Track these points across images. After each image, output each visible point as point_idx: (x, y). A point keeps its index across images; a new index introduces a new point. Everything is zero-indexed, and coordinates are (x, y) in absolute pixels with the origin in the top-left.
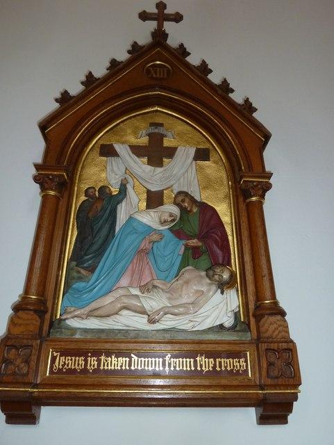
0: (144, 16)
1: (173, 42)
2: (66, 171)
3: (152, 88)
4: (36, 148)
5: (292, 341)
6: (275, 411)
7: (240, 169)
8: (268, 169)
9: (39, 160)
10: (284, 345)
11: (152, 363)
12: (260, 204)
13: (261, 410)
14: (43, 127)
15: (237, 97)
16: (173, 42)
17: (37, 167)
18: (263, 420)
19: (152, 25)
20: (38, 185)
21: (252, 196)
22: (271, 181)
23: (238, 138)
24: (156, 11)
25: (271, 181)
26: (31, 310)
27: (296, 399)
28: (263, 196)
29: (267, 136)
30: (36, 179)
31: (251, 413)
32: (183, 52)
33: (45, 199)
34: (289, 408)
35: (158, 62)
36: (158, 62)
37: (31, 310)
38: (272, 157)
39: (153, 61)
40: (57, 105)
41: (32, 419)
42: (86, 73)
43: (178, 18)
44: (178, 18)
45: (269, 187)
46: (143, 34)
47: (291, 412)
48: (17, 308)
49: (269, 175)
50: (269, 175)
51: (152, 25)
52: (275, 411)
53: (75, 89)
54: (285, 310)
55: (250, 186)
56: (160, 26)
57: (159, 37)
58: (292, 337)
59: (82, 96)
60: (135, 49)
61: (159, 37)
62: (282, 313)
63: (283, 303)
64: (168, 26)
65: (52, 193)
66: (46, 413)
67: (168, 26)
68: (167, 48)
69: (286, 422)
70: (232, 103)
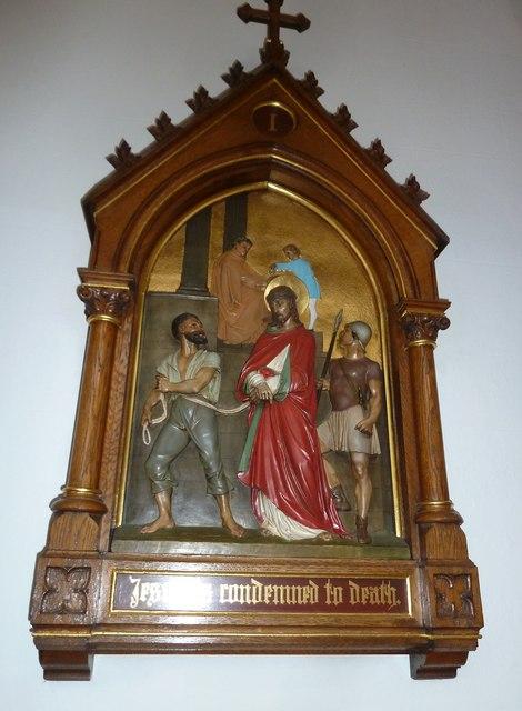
0: (246, 14)
1: (296, 69)
2: (130, 284)
3: (266, 146)
4: (79, 248)
5: (472, 565)
6: (439, 656)
7: (399, 290)
8: (442, 295)
9: (85, 263)
10: (456, 571)
11: (245, 593)
12: (430, 349)
13: (422, 661)
14: (90, 204)
15: (398, 173)
16: (296, 69)
17: (81, 272)
18: (419, 673)
19: (259, 32)
20: (83, 304)
21: (418, 339)
22: (448, 313)
23: (394, 237)
24: (265, 7)
25: (448, 313)
26: (83, 511)
27: (475, 646)
28: (434, 338)
29: (442, 241)
30: (82, 292)
31: (403, 661)
32: (310, 87)
33: (94, 327)
34: (462, 658)
35: (277, 104)
36: (277, 104)
37: (83, 511)
38: (451, 275)
39: (259, 102)
40: (110, 169)
41: (84, 674)
42: (158, 115)
43: (301, 24)
44: (301, 24)
45: (445, 324)
46: (248, 46)
47: (463, 662)
48: (60, 508)
49: (447, 304)
50: (447, 304)
51: (259, 32)
52: (439, 656)
53: (141, 142)
54: (461, 514)
55: (416, 317)
56: (273, 34)
57: (274, 55)
58: (472, 557)
59: (153, 154)
60: (235, 75)
61: (274, 55)
62: (458, 521)
63: (457, 507)
64: (287, 36)
65: (105, 317)
66: (99, 662)
67: (287, 36)
68: (287, 78)
69: (455, 675)
70: (387, 181)
